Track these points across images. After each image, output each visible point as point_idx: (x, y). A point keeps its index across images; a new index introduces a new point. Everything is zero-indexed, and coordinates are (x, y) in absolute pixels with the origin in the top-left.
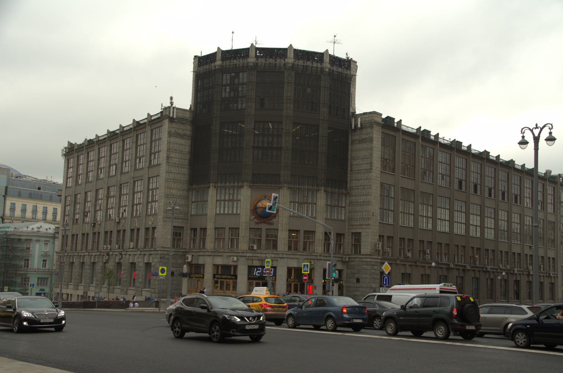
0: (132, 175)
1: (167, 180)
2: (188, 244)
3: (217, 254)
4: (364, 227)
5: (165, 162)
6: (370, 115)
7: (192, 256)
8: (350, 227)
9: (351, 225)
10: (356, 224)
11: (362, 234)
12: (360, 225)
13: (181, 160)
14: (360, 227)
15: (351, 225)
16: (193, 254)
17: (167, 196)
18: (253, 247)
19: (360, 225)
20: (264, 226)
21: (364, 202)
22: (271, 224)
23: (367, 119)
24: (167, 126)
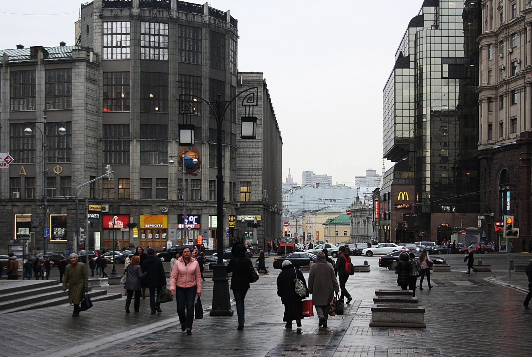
0: (8, 117)
1: (87, 127)
2: (101, 194)
3: (144, 204)
4: (253, 177)
5: (83, 108)
6: (258, 75)
7: (109, 206)
8: (239, 177)
9: (240, 175)
10: (246, 174)
11: (252, 183)
12: (249, 175)
13: (93, 107)
14: (250, 177)
15: (240, 175)
16: (112, 204)
17: (87, 145)
18: (181, 197)
19: (249, 175)
20: (190, 177)
21: (253, 154)
22: (196, 175)
23: (254, 78)
24: (83, 70)
